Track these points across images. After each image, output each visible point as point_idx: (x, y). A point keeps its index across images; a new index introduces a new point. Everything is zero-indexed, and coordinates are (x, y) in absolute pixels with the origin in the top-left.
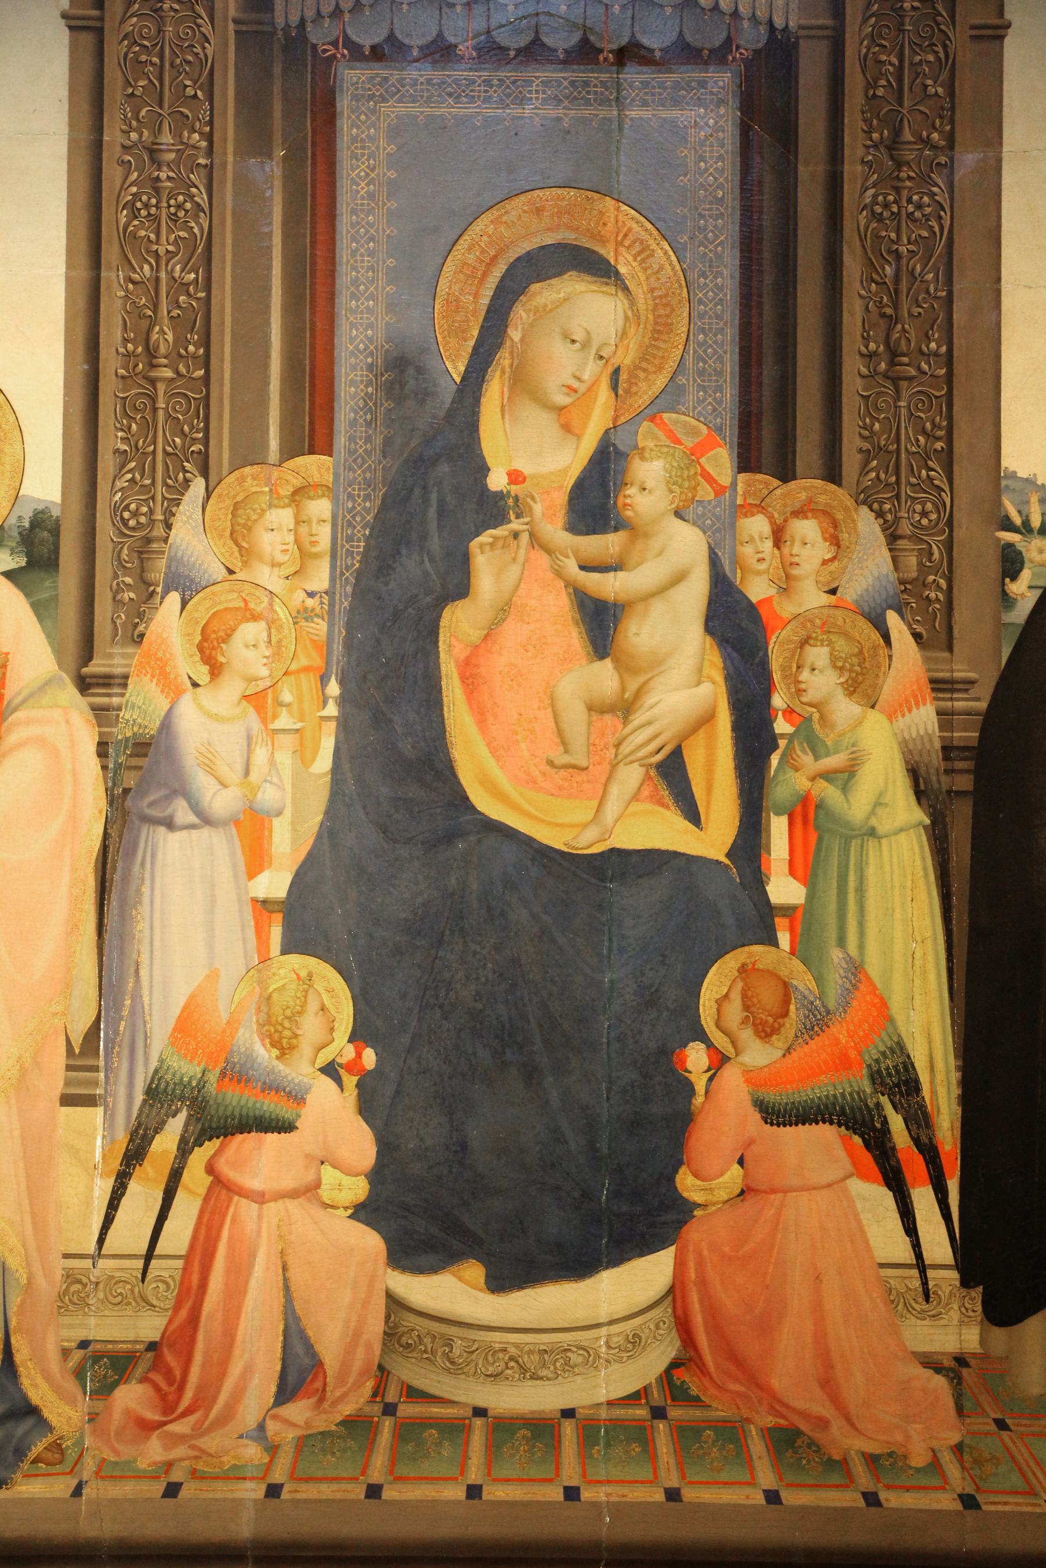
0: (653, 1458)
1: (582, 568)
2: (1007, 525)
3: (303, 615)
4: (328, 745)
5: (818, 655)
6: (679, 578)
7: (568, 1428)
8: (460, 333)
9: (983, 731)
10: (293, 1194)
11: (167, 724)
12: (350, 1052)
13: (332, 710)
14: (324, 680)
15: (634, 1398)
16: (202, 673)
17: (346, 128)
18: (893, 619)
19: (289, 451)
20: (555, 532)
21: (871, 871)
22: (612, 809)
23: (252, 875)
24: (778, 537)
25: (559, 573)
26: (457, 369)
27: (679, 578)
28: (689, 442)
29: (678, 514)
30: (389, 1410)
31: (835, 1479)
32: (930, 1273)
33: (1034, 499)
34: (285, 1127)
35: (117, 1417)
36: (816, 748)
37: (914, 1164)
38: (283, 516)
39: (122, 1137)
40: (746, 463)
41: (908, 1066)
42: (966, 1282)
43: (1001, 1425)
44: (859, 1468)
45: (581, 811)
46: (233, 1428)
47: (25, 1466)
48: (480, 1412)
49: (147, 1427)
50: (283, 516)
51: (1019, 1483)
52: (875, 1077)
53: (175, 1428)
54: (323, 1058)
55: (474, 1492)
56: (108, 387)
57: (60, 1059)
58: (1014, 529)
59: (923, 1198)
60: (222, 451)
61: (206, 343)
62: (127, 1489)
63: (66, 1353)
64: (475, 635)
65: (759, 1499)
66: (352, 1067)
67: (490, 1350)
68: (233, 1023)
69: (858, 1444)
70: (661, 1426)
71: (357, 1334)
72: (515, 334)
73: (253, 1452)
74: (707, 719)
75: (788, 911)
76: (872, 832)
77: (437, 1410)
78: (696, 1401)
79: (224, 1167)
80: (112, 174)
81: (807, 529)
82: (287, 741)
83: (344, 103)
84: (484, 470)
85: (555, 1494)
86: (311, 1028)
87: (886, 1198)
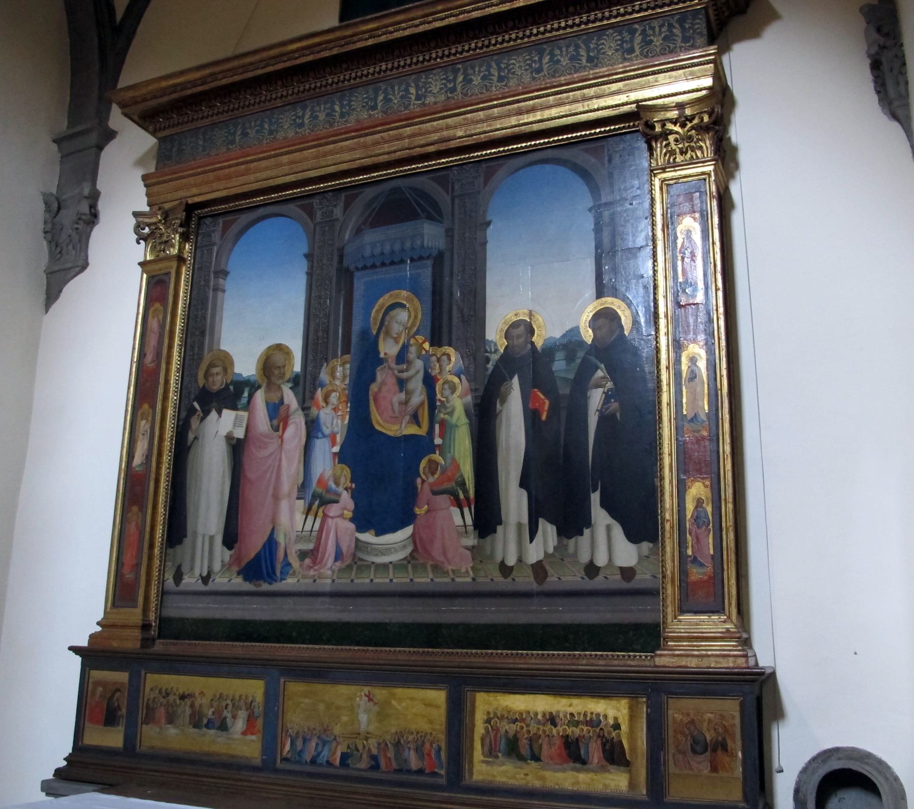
0: (408, 572)
1: (399, 372)
2: (486, 352)
3: (344, 389)
4: (347, 417)
5: (446, 386)
6: (418, 372)
7: (391, 566)
8: (375, 324)
9: (482, 400)
10: (338, 517)
11: (318, 417)
12: (350, 485)
13: (348, 410)
14: (347, 404)
15: (404, 559)
16: (324, 405)
17: (356, 285)
18: (463, 377)
19: (342, 354)
20: (393, 365)
21: (456, 435)
22: (403, 425)
23: (333, 447)
24: (439, 360)
25: (394, 374)
26: (374, 332)
27: (418, 372)
28: (421, 341)
29: (418, 358)
30: (356, 563)
31: (446, 575)
32: (468, 528)
33: (493, 344)
34: (337, 502)
35: (305, 566)
36: (446, 408)
37: (465, 502)
38: (341, 368)
39: (307, 505)
40: (432, 345)
41: (464, 480)
42: (475, 529)
43: (481, 561)
44: (451, 573)
45: (396, 427)
46: (327, 567)
47: (289, 576)
48: (373, 563)
49: (310, 568)
50: (341, 368)
51: (484, 575)
52: (457, 483)
53: (316, 568)
54: (345, 486)
55: (372, 580)
56: (310, 345)
57: (296, 490)
58: (488, 352)
59: (466, 510)
60: (330, 356)
61: (328, 334)
62: (307, 581)
63: (296, 552)
64: (376, 389)
65: (429, 580)
66: (351, 488)
67: (375, 549)
68: (328, 480)
69: (450, 568)
70: (410, 565)
71: (349, 546)
72: (386, 323)
73: (330, 572)
74: (422, 404)
75: (438, 446)
76: (457, 426)
77: (365, 563)
78: (417, 559)
79: (326, 512)
80: (313, 301)
81: (445, 358)
82: (340, 417)
83: (355, 281)
84: (379, 353)
85: (388, 581)
86: (343, 480)
87: (458, 510)
